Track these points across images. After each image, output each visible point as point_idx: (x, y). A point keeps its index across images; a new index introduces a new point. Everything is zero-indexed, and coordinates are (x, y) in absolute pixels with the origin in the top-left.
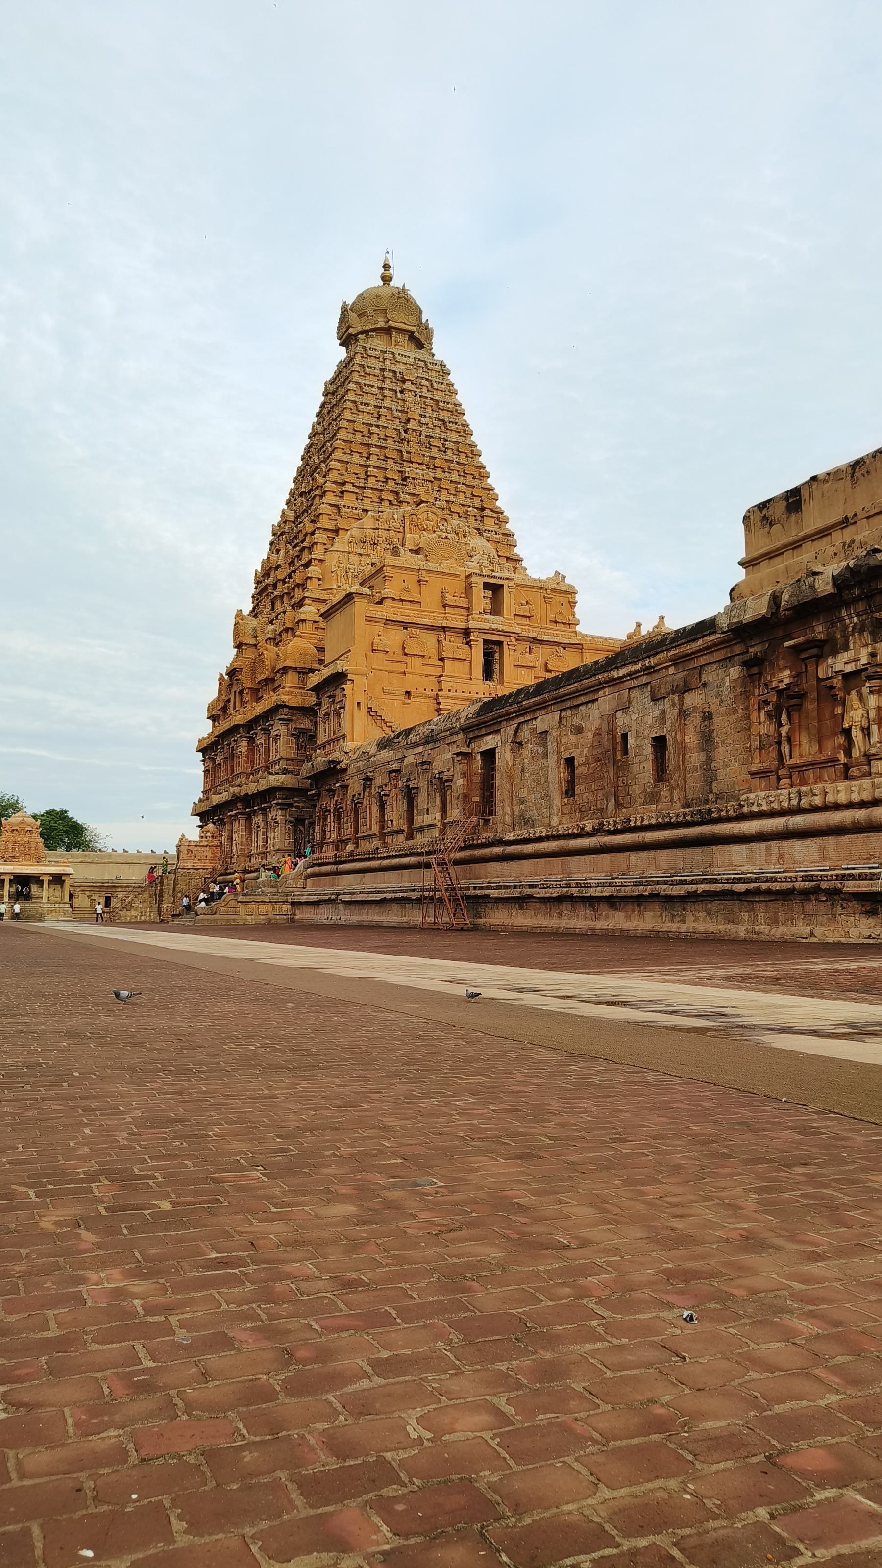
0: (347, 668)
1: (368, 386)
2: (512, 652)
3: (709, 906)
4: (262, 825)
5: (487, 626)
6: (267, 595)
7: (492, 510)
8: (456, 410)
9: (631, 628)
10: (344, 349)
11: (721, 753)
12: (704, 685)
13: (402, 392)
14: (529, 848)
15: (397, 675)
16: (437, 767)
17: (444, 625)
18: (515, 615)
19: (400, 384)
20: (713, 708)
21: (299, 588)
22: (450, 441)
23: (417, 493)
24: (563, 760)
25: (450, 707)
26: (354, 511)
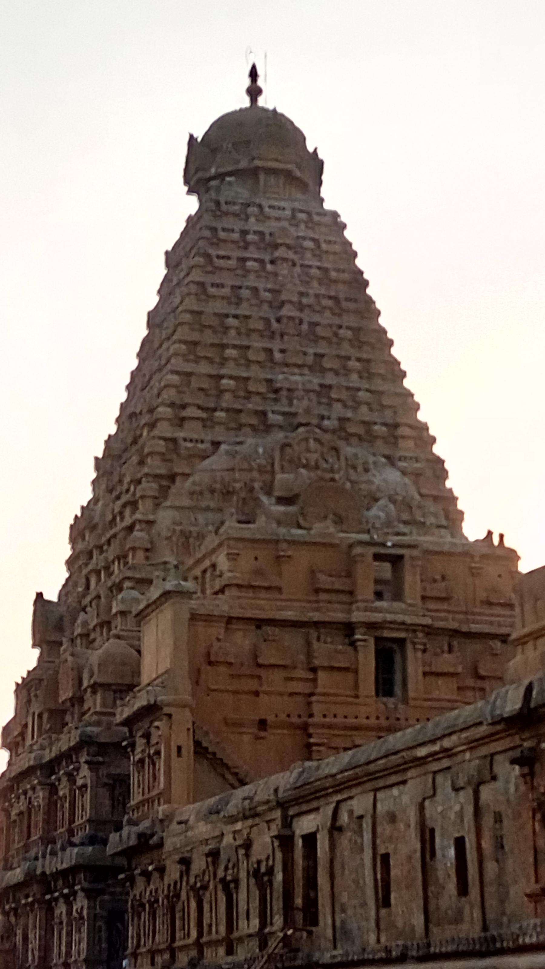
0: (163, 697)
1: (223, 257)
2: (419, 654)
5: (377, 617)
6: (80, 567)
7: (410, 426)
11: (510, 864)
12: (494, 778)
13: (272, 262)
15: (244, 696)
17: (315, 620)
19: (269, 250)
20: (502, 808)
21: (119, 563)
22: (348, 328)
23: (292, 410)
25: (326, 741)
26: (200, 446)
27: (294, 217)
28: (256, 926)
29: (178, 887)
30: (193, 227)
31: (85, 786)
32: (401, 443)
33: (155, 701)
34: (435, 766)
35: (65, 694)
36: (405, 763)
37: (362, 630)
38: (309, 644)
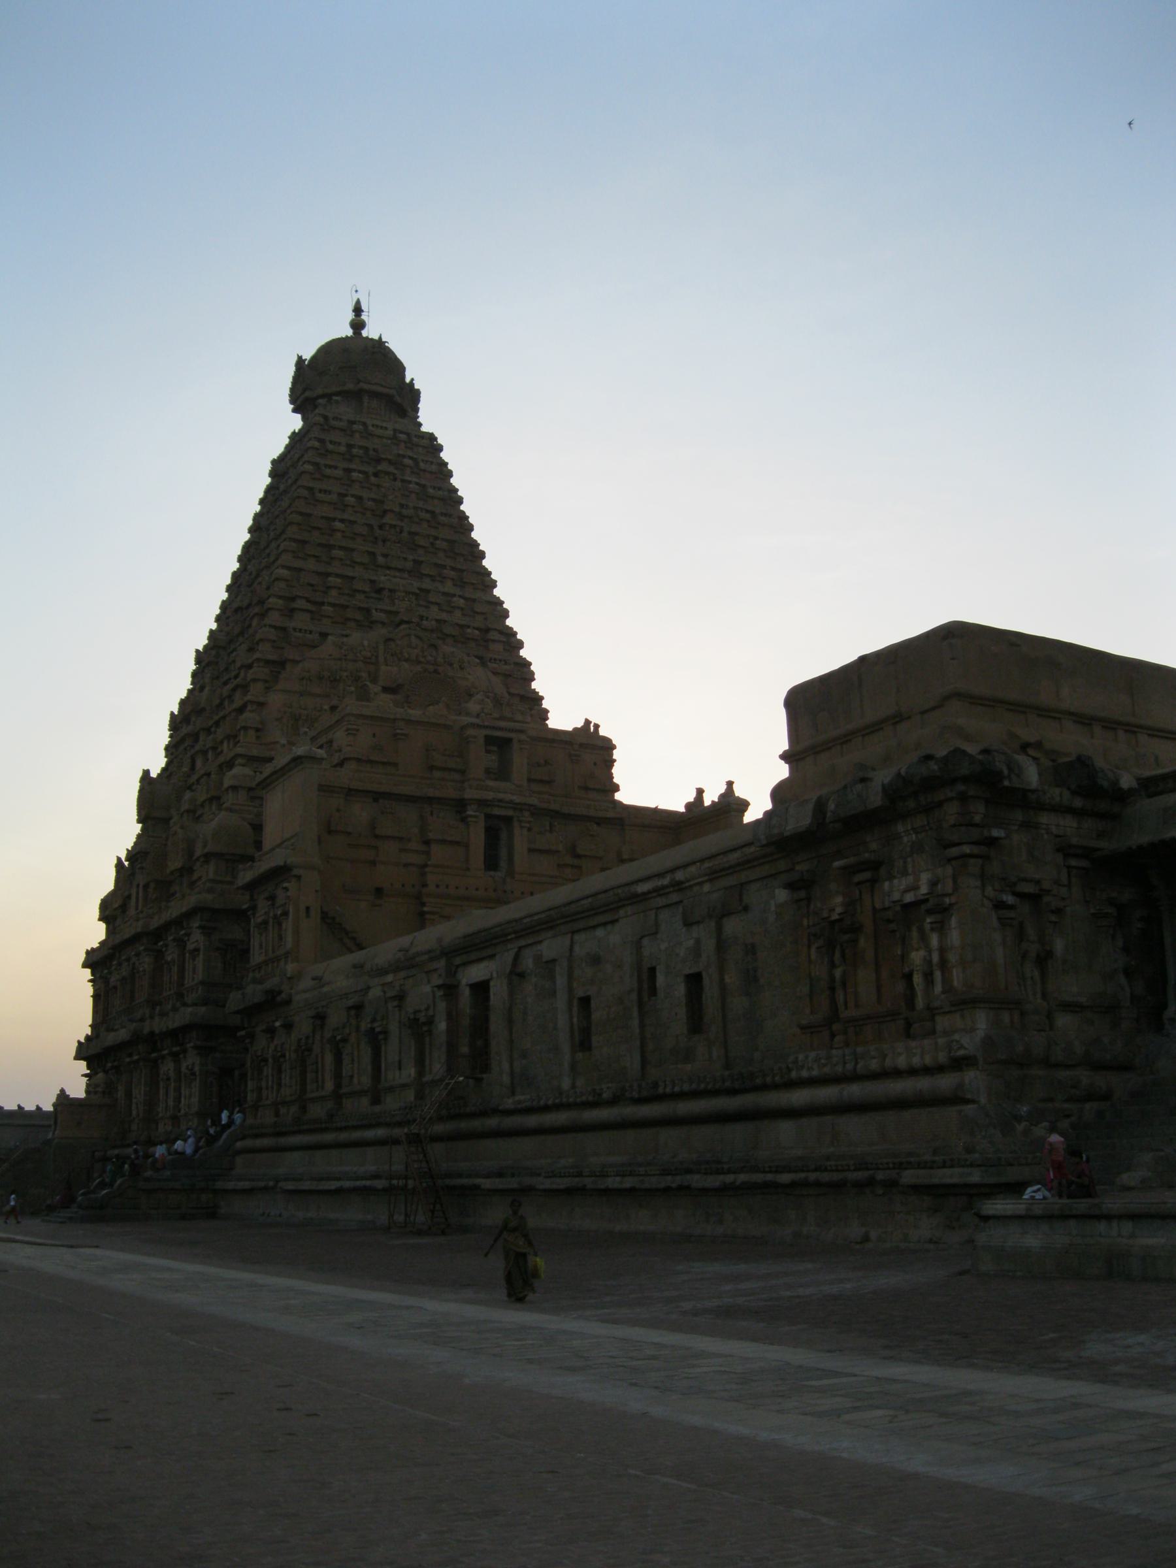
1: (330, 467)
2: (525, 832)
4: (172, 1074)
5: (490, 795)
6: (185, 749)
9: (691, 797)
10: (298, 417)
12: (746, 909)
13: (376, 475)
14: (532, 1121)
22: (443, 539)
23: (393, 609)
24: (575, 1002)
26: (308, 636)
27: (394, 437)
28: (410, 1075)
30: (300, 440)
31: (197, 950)
32: (492, 646)
33: (285, 862)
34: (660, 901)
35: (174, 863)
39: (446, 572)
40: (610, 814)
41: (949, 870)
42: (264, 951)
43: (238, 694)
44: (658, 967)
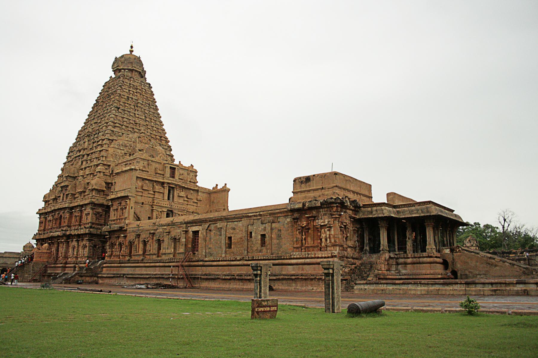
1: (125, 89)
3: (283, 282)
4: (76, 246)
5: (170, 182)
7: (164, 138)
8: (153, 101)
10: (113, 72)
12: (279, 222)
13: (136, 93)
14: (215, 263)
16: (173, 234)
17: (156, 180)
18: (179, 179)
24: (227, 238)
28: (171, 251)
29: (134, 240)
32: (162, 141)
34: (255, 218)
36: (244, 216)
37: (166, 184)
38: (153, 185)
39: (152, 121)
40: (196, 189)
41: (332, 219)
42: (116, 216)
43: (99, 147)
44: (253, 232)
